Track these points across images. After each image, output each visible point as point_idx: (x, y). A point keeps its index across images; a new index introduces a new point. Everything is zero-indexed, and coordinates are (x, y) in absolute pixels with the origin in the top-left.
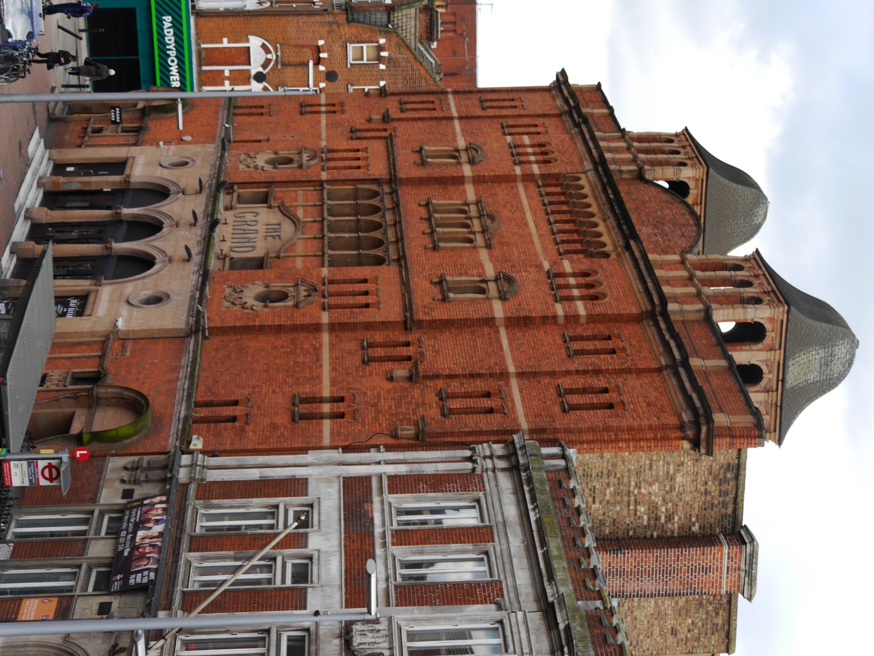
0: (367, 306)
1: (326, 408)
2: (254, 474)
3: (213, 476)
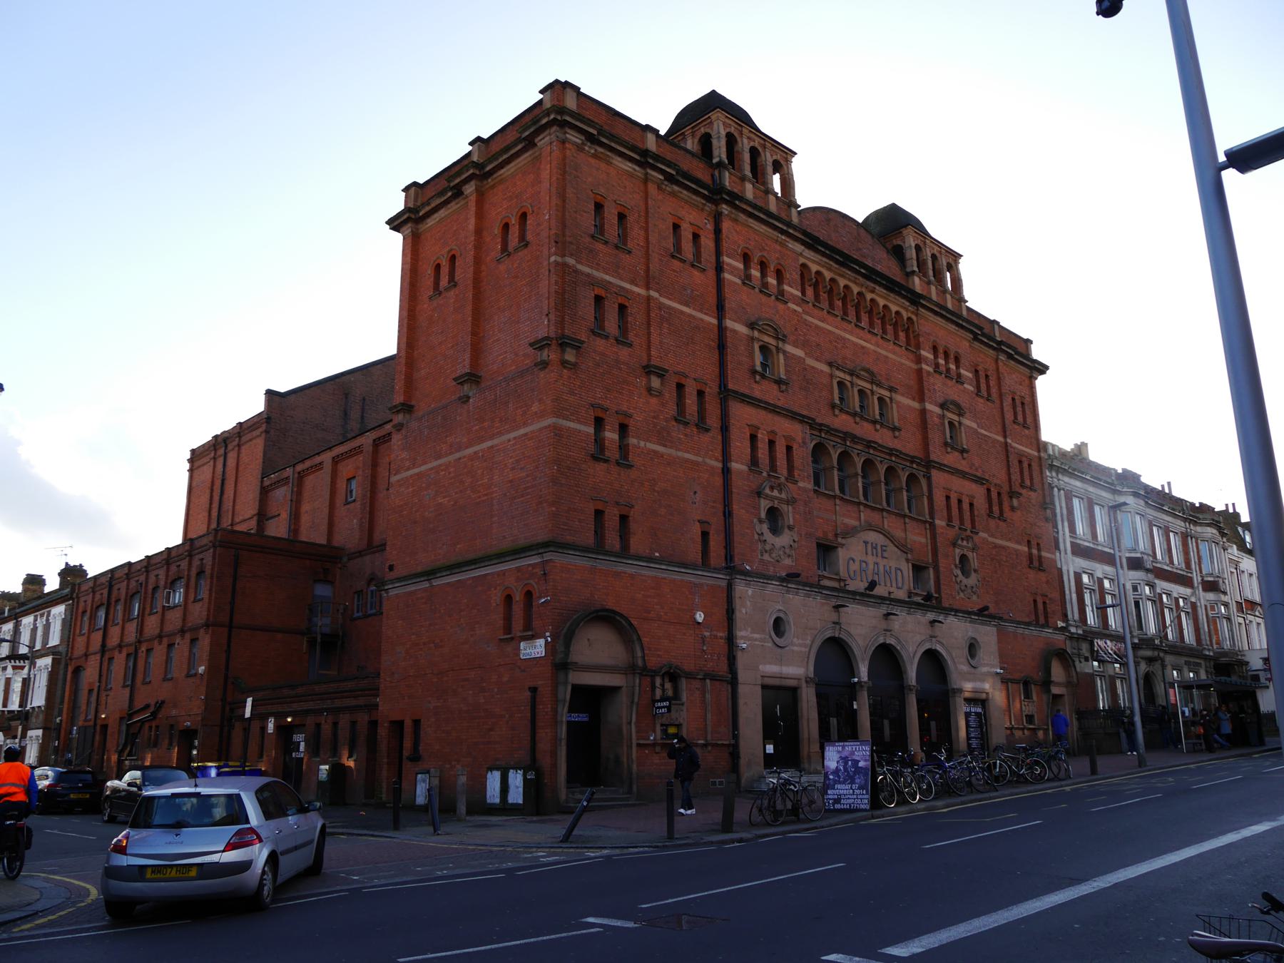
0: (971, 505)
1: (1035, 551)
2: (1074, 596)
3: (1077, 616)
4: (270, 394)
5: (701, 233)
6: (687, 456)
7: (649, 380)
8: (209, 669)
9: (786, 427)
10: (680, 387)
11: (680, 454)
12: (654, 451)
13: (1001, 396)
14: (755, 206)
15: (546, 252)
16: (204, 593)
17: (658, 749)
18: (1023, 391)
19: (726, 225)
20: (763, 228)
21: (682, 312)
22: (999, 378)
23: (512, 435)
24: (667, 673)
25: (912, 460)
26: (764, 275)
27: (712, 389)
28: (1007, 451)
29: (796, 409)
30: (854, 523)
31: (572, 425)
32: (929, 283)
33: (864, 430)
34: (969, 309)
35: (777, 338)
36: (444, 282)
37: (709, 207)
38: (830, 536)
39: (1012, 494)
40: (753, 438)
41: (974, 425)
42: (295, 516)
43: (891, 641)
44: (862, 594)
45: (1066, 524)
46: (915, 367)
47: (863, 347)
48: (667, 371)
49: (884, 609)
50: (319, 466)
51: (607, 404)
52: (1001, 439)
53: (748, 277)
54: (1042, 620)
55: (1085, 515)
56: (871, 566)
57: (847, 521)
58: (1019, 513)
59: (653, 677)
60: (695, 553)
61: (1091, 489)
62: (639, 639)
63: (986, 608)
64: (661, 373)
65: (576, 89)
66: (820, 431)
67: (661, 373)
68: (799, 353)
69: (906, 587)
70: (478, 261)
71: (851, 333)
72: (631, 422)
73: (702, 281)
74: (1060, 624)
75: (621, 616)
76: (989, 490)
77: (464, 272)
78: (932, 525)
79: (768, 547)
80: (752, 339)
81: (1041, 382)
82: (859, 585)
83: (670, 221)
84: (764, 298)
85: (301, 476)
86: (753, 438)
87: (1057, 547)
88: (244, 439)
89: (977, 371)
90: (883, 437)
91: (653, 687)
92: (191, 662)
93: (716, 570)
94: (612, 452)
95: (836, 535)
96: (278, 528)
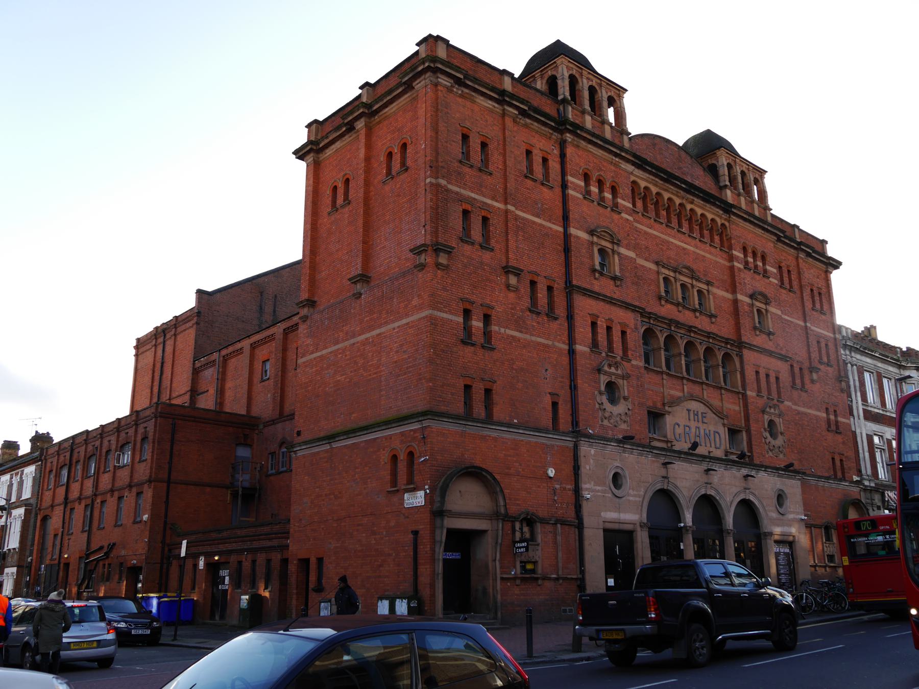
0: (777, 378)
1: (832, 417)
2: (867, 454)
3: (869, 472)
4: (200, 292)
5: (549, 157)
6: (539, 340)
7: (508, 279)
8: (152, 517)
9: (620, 315)
10: (533, 283)
11: (533, 338)
12: (513, 337)
13: (801, 287)
14: (593, 135)
15: (422, 175)
16: (147, 455)
17: (518, 582)
18: (821, 284)
19: (569, 151)
20: (600, 152)
21: (534, 223)
22: (799, 273)
23: (396, 324)
24: (524, 519)
25: (727, 341)
26: (601, 191)
27: (559, 285)
28: (807, 333)
29: (629, 301)
30: (680, 394)
31: (445, 315)
32: (739, 195)
33: (686, 317)
34: (773, 216)
35: (613, 243)
36: (340, 200)
37: (556, 135)
38: (659, 405)
39: (812, 369)
40: (594, 325)
41: (779, 312)
42: (221, 392)
43: (712, 493)
44: (685, 453)
45: (859, 394)
46: (728, 264)
47: (684, 249)
48: (522, 271)
49: (705, 466)
50: (240, 351)
51: (473, 298)
52: (802, 323)
53: (588, 193)
54: (839, 475)
55: (875, 386)
56: (693, 430)
57: (673, 392)
58: (818, 385)
59: (513, 522)
60: (546, 419)
61: (880, 365)
62: (502, 491)
63: (791, 465)
64: (518, 273)
65: (446, 42)
66: (649, 318)
67: (518, 273)
68: (632, 254)
69: (723, 447)
70: (367, 183)
71: (674, 237)
72: (493, 313)
73: (551, 196)
74: (855, 478)
75: (487, 471)
76: (792, 366)
77: (357, 192)
78: (744, 396)
79: (607, 415)
80: (592, 243)
81: (835, 276)
82: (684, 446)
83: (523, 148)
84: (601, 210)
85: (225, 360)
86: (594, 325)
87: (851, 414)
88: (179, 329)
89: (780, 267)
90: (702, 323)
91: (514, 531)
92: (137, 512)
93: (564, 434)
94: (478, 338)
95: (664, 404)
96: (207, 402)
